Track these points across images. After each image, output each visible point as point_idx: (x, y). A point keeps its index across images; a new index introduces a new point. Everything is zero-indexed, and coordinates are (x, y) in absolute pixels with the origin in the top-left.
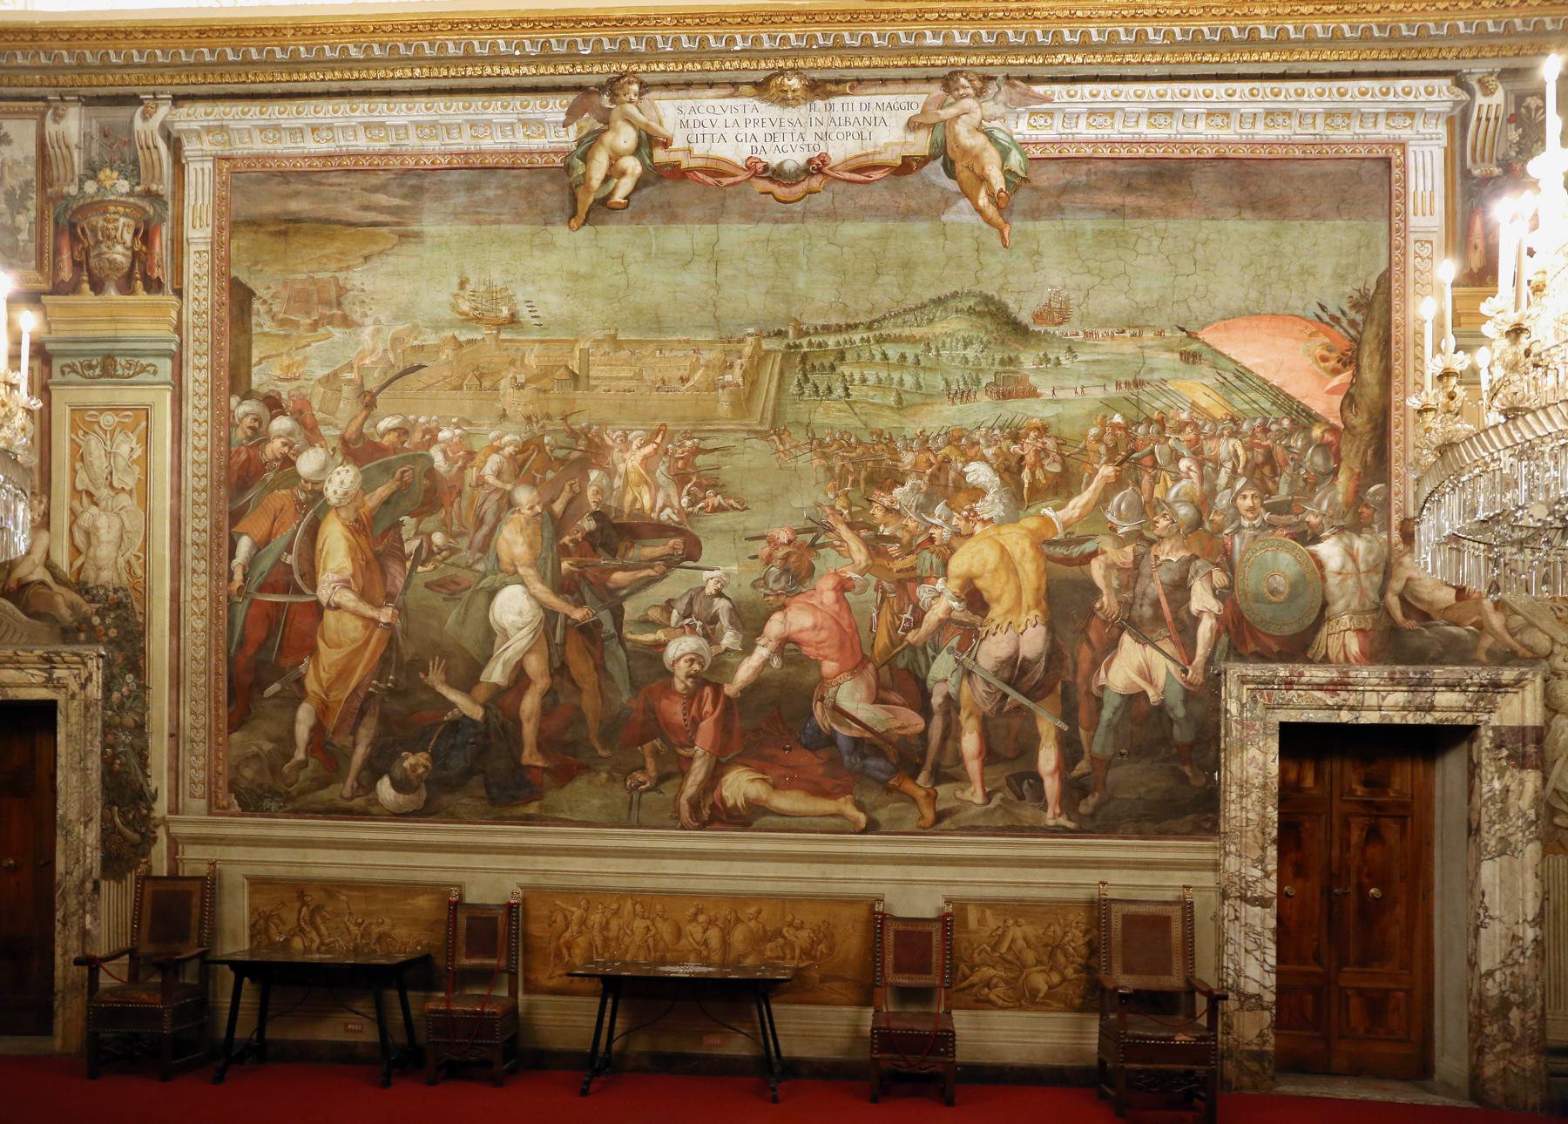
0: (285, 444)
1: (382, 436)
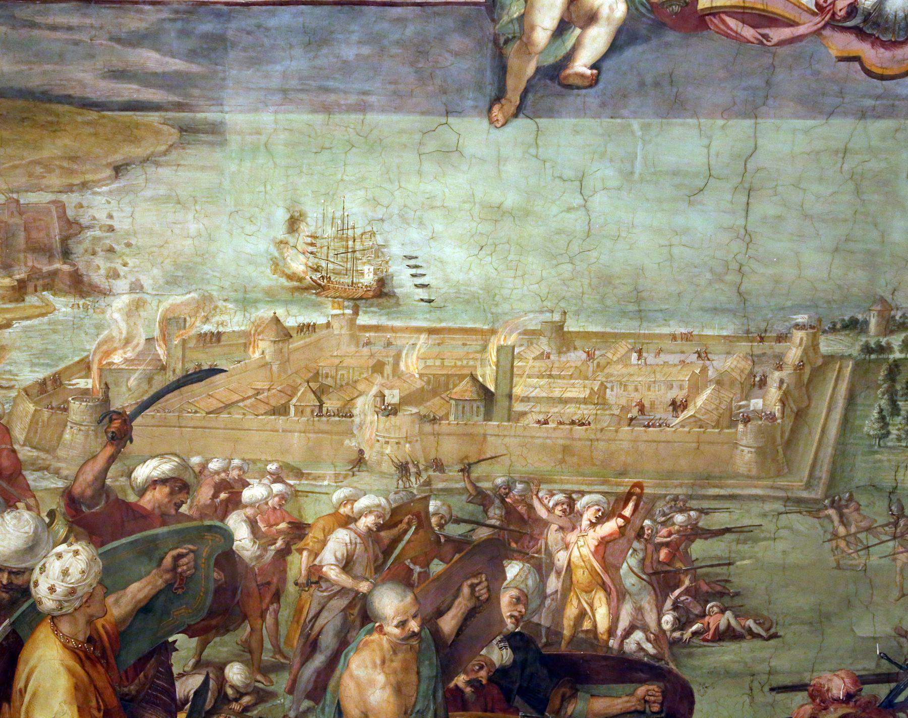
1: (142, 492)
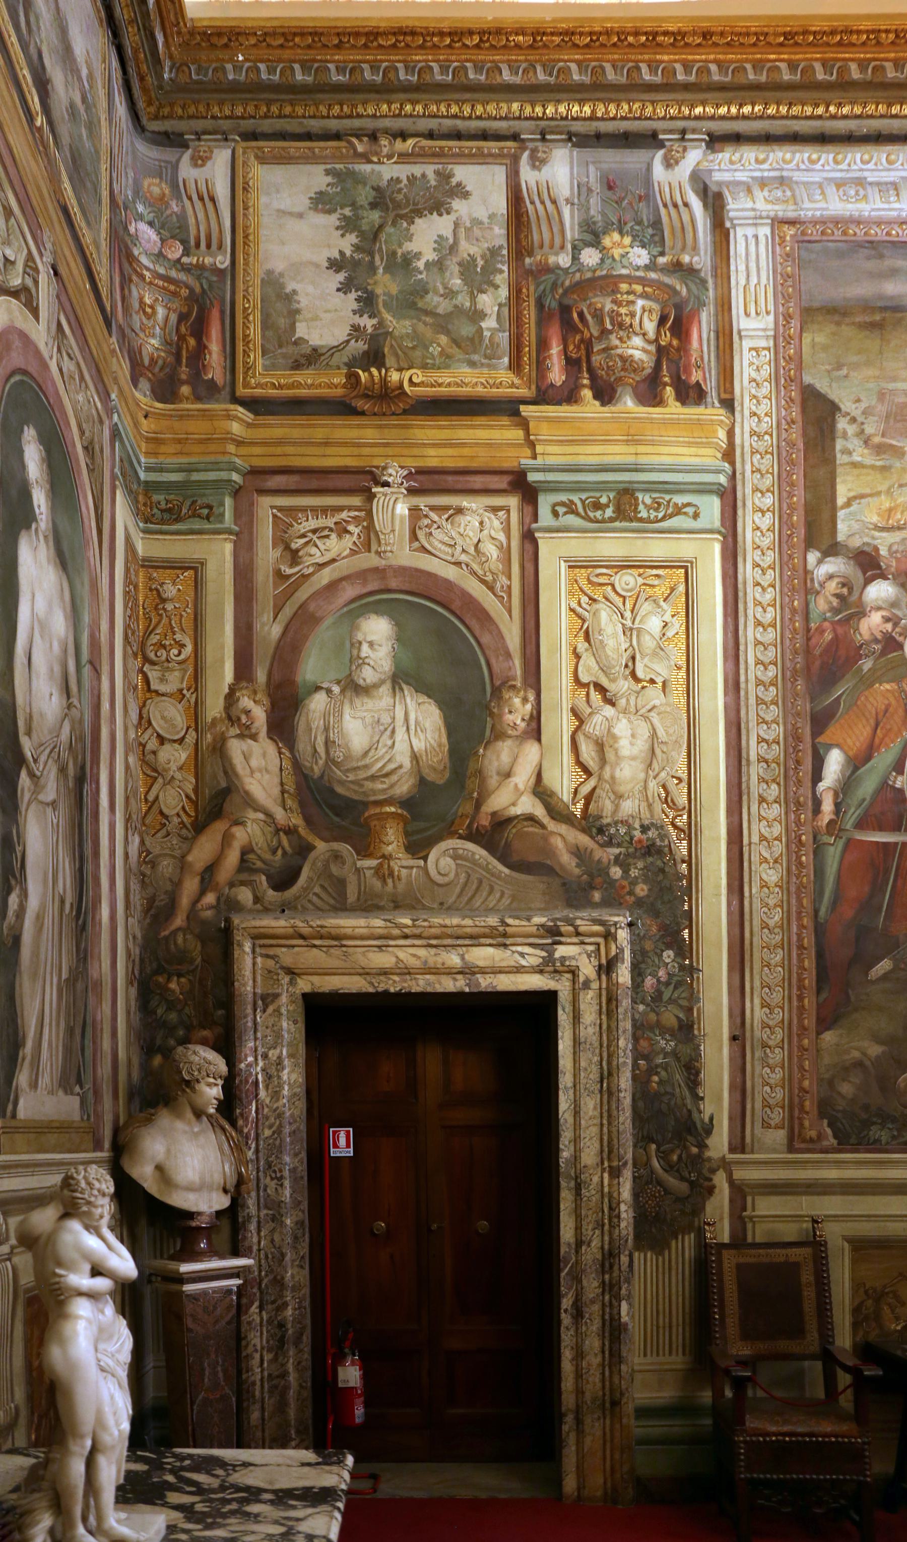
0: (887, 620)
